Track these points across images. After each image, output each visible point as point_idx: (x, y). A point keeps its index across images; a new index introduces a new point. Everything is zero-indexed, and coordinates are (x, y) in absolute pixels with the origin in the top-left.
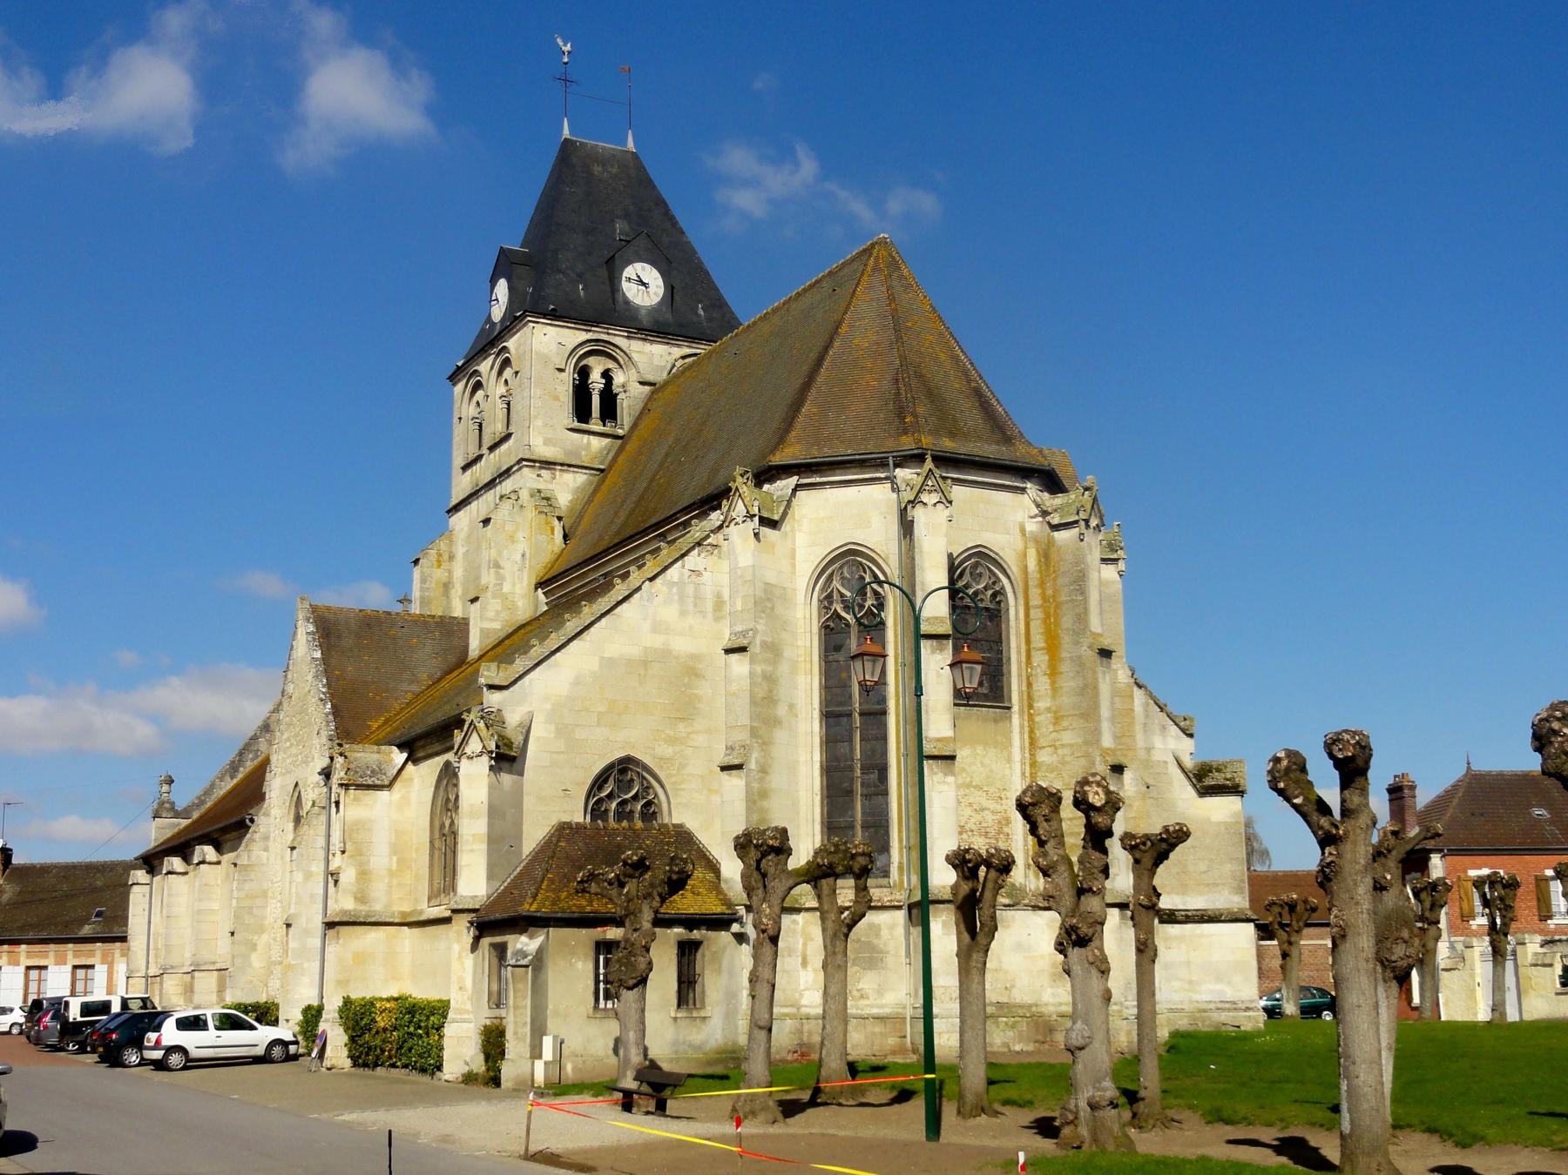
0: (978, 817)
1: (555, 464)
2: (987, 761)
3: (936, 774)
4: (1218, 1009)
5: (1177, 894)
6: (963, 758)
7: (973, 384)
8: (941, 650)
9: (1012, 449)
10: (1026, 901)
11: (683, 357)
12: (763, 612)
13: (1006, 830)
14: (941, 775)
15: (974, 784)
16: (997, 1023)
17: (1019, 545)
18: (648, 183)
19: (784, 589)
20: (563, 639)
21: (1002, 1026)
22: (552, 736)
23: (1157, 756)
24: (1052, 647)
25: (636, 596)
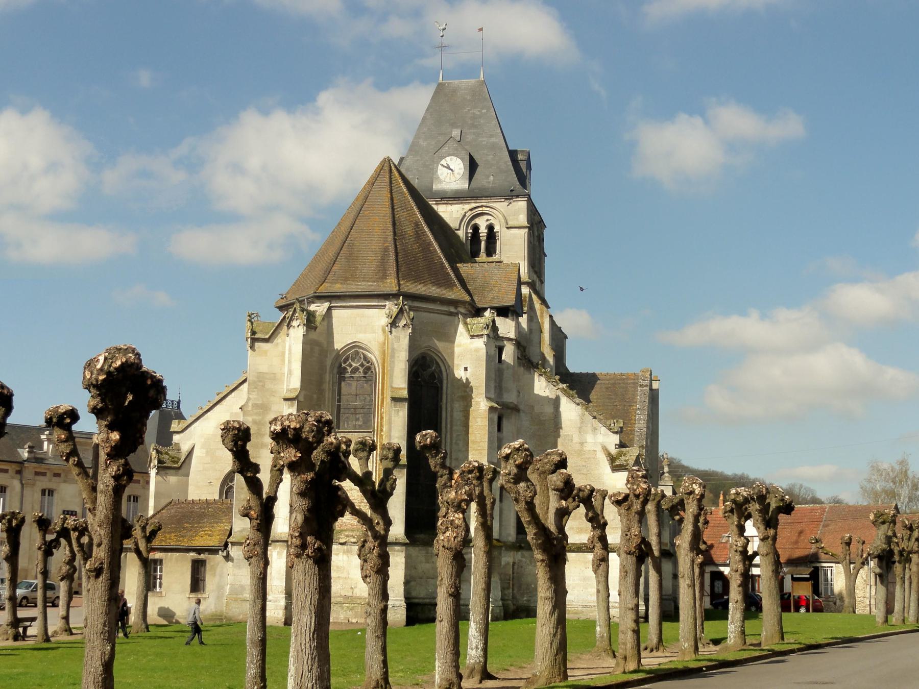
8: (292, 406)
11: (471, 210)
12: (256, 388)
19: (275, 374)
22: (204, 455)
23: (588, 447)
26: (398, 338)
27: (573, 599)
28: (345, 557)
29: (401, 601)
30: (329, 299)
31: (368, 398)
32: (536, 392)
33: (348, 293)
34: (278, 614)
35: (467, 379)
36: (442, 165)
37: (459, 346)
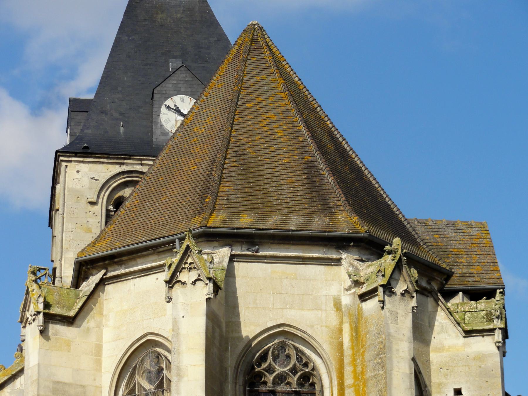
7: (307, 158)
9: (327, 219)
17: (333, 320)
19: (83, 387)
30: (229, 241)
36: (168, 107)
37: (441, 349)
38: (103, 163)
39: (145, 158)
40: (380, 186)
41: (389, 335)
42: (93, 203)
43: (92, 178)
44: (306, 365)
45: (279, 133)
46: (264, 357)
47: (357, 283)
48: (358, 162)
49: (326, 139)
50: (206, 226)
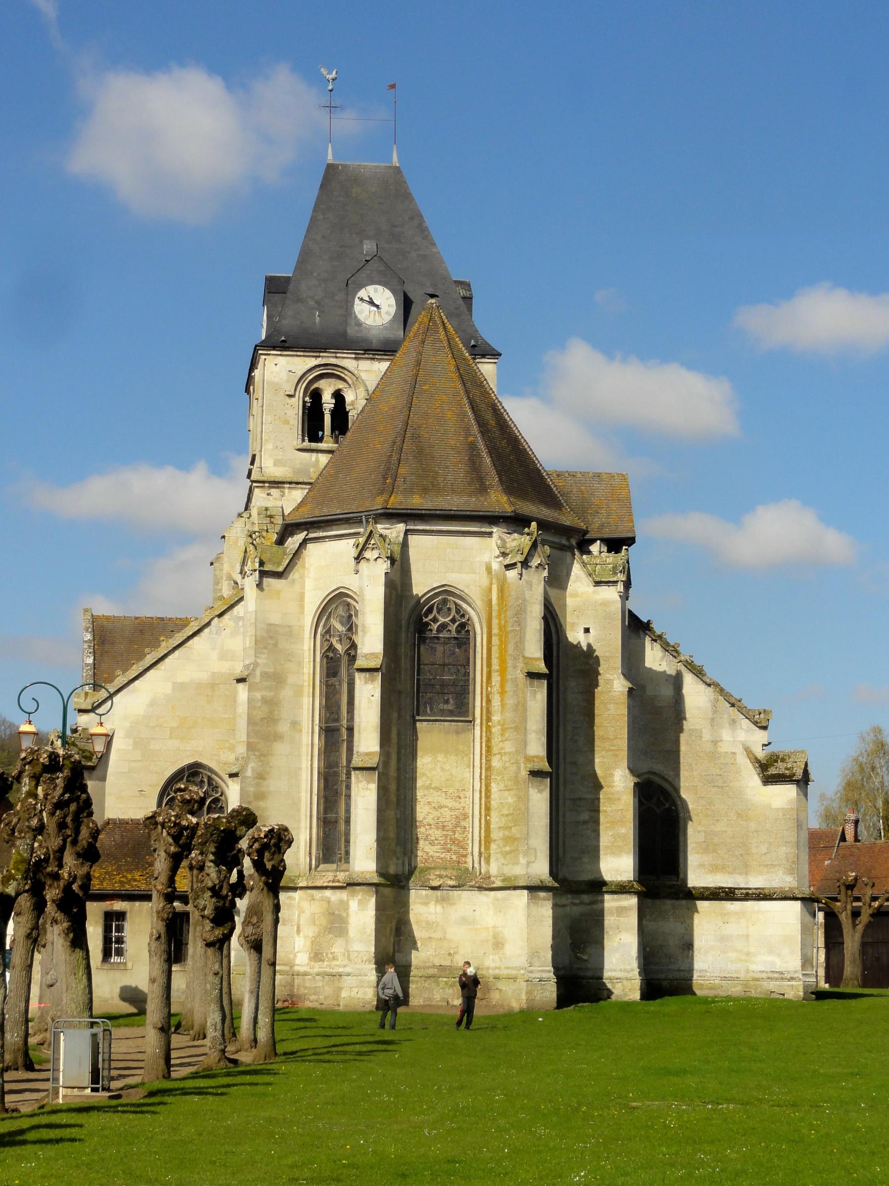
0: (437, 814)
1: (284, 483)
2: (447, 767)
3: (361, 782)
4: (769, 978)
5: (740, 874)
6: (423, 765)
7: (471, 439)
8: (373, 681)
10: (473, 883)
12: (265, 648)
13: (463, 823)
14: (364, 782)
15: (433, 786)
16: (438, 983)
17: (485, 582)
18: (405, 196)
19: (290, 627)
20: (141, 669)
21: (442, 985)
22: (131, 748)
23: (724, 748)
24: (503, 672)
25: (206, 630)
26: (530, 584)
27: (706, 968)
28: (439, 909)
29: (549, 972)
31: (462, 670)
32: (647, 665)
33: (438, 512)
34: (365, 994)
35: (589, 646)
36: (361, 299)
38: (300, 356)
39: (339, 351)
40: (533, 453)
41: (525, 600)
42: (290, 396)
43: (289, 371)
44: (463, 616)
45: (449, 414)
46: (430, 610)
47: (504, 554)
48: (516, 432)
49: (489, 417)
50: (386, 508)
